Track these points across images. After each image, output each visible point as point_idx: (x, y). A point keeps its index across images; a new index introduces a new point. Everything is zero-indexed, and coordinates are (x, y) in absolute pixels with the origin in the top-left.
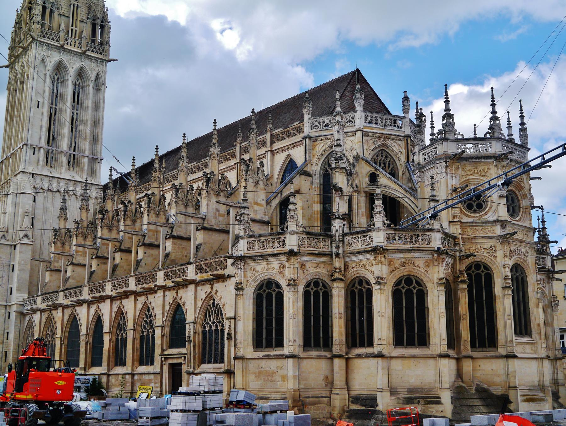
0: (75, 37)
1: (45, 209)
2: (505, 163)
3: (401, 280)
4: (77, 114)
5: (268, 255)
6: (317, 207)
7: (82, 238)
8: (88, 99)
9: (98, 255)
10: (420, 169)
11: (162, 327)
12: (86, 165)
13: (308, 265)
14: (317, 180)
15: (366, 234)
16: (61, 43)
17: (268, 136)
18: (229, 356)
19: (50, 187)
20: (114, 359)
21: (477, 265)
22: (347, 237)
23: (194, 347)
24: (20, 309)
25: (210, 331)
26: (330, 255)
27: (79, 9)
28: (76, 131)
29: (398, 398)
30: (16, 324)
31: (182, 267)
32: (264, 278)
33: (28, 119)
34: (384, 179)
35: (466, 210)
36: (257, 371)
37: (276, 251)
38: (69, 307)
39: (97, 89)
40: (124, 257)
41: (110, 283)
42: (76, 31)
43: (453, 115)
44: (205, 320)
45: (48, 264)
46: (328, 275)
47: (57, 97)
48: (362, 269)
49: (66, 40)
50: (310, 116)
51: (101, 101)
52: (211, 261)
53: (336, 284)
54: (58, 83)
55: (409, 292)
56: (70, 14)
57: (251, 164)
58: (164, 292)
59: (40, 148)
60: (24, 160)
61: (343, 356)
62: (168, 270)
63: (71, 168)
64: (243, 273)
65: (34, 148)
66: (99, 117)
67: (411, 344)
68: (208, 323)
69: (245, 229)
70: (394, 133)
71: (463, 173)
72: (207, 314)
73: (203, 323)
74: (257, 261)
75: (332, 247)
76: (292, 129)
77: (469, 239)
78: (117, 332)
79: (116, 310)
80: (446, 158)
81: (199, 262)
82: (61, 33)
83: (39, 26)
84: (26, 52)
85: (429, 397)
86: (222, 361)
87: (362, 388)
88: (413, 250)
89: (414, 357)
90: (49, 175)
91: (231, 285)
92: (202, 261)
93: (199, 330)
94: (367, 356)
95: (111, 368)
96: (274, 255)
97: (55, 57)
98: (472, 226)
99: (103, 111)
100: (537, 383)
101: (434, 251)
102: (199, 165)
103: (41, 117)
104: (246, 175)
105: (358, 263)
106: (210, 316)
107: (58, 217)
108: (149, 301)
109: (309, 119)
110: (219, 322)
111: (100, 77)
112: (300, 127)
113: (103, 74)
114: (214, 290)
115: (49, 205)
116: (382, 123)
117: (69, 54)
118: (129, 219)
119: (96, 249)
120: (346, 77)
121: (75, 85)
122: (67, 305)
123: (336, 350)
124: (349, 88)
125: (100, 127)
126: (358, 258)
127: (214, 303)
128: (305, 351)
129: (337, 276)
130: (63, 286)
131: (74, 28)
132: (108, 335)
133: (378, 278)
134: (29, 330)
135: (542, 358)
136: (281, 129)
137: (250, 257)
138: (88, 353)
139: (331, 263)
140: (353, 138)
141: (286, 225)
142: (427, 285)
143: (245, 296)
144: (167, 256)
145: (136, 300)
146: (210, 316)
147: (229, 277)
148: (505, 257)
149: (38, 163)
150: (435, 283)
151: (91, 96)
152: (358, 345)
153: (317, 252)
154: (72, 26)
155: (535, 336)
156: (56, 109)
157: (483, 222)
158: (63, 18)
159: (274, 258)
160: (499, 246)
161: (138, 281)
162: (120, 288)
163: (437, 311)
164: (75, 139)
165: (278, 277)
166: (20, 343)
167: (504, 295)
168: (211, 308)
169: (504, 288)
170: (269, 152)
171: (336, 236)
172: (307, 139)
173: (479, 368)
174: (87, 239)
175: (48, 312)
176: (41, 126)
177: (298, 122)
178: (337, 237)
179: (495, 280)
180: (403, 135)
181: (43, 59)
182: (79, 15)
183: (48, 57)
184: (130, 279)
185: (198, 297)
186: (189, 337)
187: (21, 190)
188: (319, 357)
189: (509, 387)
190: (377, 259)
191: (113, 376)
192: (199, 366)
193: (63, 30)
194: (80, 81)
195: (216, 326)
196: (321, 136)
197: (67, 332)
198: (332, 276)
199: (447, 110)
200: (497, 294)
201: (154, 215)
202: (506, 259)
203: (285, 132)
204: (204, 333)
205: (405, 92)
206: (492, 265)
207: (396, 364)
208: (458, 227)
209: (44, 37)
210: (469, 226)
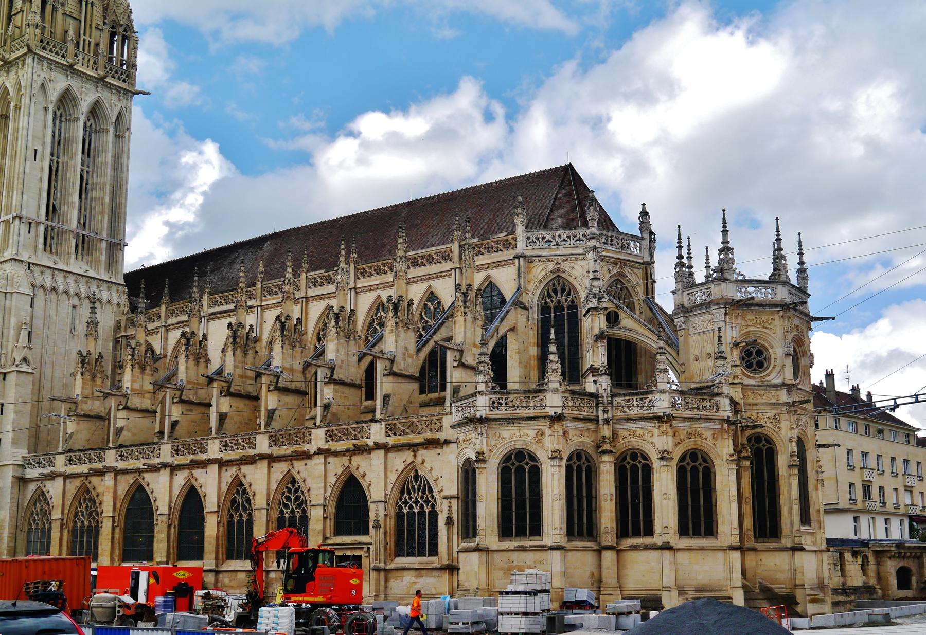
0: (89, 52)
1: (47, 318)
2: (792, 312)
3: (686, 455)
4: (88, 172)
6: (534, 351)
7: (139, 370)
8: (106, 151)
9: (183, 398)
10: (684, 312)
11: (324, 506)
12: (104, 253)
13: (571, 433)
14: (535, 315)
15: (645, 396)
16: (70, 60)
17: (455, 247)
18: (450, 548)
19: (54, 285)
20: (225, 550)
21: (758, 438)
22: (616, 399)
23: (385, 533)
24: (18, 474)
25: (411, 514)
26: (596, 420)
27: (95, 8)
28: (86, 199)
29: (687, 599)
30: (13, 495)
31: (360, 425)
32: (514, 447)
33: (21, 176)
34: (626, 321)
35: (746, 369)
36: (506, 566)
37: (532, 413)
38: (128, 473)
39: (118, 136)
40: (233, 405)
41: (217, 441)
42: (90, 42)
43: (732, 249)
44: (401, 499)
45: (73, 406)
46: (593, 446)
47: (59, 144)
48: (638, 439)
49: (76, 55)
50: (523, 228)
51: (125, 156)
52: (414, 420)
53: (605, 458)
54: (61, 122)
55: (694, 469)
56: (81, 16)
57: (469, 292)
58: (325, 458)
59: (38, 223)
60: (15, 242)
61: (615, 547)
62: (334, 428)
63: (80, 256)
64: (484, 440)
65: (30, 223)
66: (122, 180)
67: (697, 533)
68: (406, 503)
69: (486, 383)
70: (631, 259)
71: (743, 323)
72: (404, 489)
73: (397, 503)
74: (504, 425)
75: (597, 411)
76: (494, 242)
77: (750, 405)
78: (229, 511)
79: (230, 480)
80: (726, 304)
81: (392, 419)
82: (69, 44)
83: (38, 31)
84: (8, 68)
85: (719, 598)
86: (434, 551)
87: (639, 586)
88: (701, 418)
89: (702, 549)
90: (52, 266)
91: (451, 453)
92: (397, 419)
93: (392, 511)
94: (647, 548)
95: (220, 562)
96: (530, 419)
97: (60, 83)
98: (754, 390)
99: (128, 170)
100: (816, 581)
101: (724, 420)
102: (329, 275)
103: (39, 176)
104: (465, 308)
105: (632, 432)
106: (409, 493)
107: (86, 335)
108: (297, 469)
109: (523, 232)
110: (427, 502)
111: (124, 117)
112: (507, 240)
113: (127, 114)
114: (419, 459)
115: (53, 313)
116: (618, 244)
117: (79, 78)
118: (239, 350)
119: (178, 389)
120: (554, 172)
121: (85, 127)
122: (126, 470)
123: (608, 538)
124: (564, 191)
125: (124, 196)
126: (632, 425)
127: (417, 477)
128: (569, 541)
129: (606, 447)
130: (115, 441)
131: (87, 38)
132: (215, 516)
133: (663, 452)
134: (35, 505)
135: (822, 551)
136: (476, 240)
137: (495, 419)
138: (172, 540)
139: (596, 431)
140: (583, 263)
141: (546, 381)
142: (715, 462)
143: (488, 470)
144: (326, 407)
145: (270, 467)
146: (409, 493)
147: (447, 442)
148: (792, 428)
149: (36, 246)
150: (725, 459)
151: (110, 145)
152: (630, 534)
153: (582, 417)
154: (84, 35)
155: (814, 524)
156: (58, 163)
157: (767, 386)
158: (69, 20)
160: (784, 417)
161: (273, 441)
162: (237, 449)
163: (726, 493)
164: (85, 211)
165: (534, 446)
166: (19, 524)
167: (791, 475)
169: (791, 467)
170: (457, 270)
171: (603, 397)
172: (521, 259)
173: (760, 563)
174: (146, 372)
175: (82, 479)
176: (40, 189)
177: (505, 234)
178: (605, 399)
179: (779, 457)
180: (641, 261)
181: (43, 84)
182: (94, 18)
183: (50, 80)
184: (258, 437)
185: (389, 467)
186: (376, 521)
187: (12, 286)
188: (585, 549)
189: (796, 585)
190: (661, 428)
191: (226, 574)
192: (392, 560)
193: (72, 39)
194: (92, 121)
195: (422, 507)
196: (540, 256)
197: (124, 509)
198: (599, 447)
199: (725, 242)
200: (780, 473)
201: (289, 348)
202: (793, 431)
203: (482, 244)
204: (399, 516)
205: (644, 205)
206: (776, 438)
207: (683, 557)
208: (740, 390)
209: (44, 48)
210: (750, 389)
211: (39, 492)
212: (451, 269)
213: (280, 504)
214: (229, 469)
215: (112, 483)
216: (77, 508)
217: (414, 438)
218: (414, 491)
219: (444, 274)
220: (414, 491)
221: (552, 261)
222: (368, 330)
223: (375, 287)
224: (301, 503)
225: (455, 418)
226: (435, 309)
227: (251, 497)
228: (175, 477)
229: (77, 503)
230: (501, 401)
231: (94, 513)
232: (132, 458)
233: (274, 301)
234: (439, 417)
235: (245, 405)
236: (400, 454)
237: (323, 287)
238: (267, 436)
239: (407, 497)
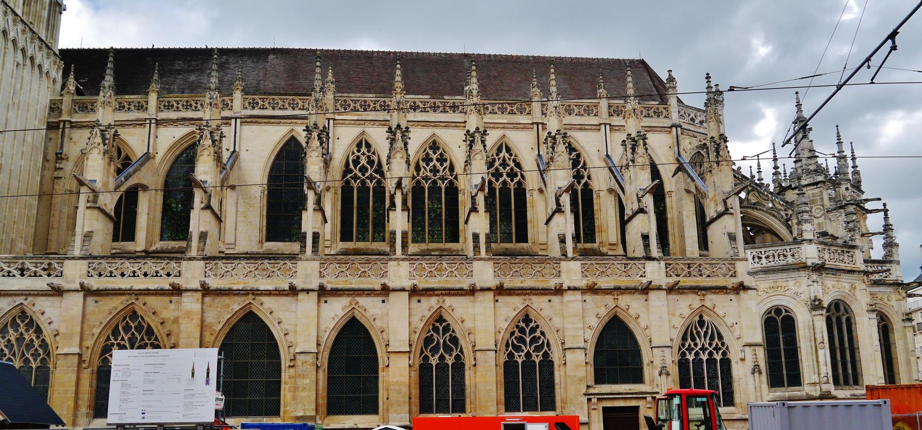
5: (844, 270)
20: (418, 401)
25: (698, 362)
44: (683, 345)
62: (593, 262)
72: (688, 334)
73: (680, 349)
78: (422, 352)
93: (677, 358)
106: (693, 339)
127: (701, 323)
146: (693, 339)
159: (847, 275)
165: (850, 298)
168: (696, 329)
177: (657, 103)
204: (683, 364)
211: (16, 312)
212: (600, 125)
213: (507, 345)
214: (423, 299)
215: (198, 306)
216: (108, 339)
217: (702, 281)
219: (589, 127)
221: (696, 137)
223: (501, 126)
224: (542, 346)
225: (750, 265)
228: (323, 305)
229: (110, 332)
230: (760, 255)
233: (355, 118)
234: (733, 262)
236: (684, 296)
237: (427, 114)
239: (692, 344)
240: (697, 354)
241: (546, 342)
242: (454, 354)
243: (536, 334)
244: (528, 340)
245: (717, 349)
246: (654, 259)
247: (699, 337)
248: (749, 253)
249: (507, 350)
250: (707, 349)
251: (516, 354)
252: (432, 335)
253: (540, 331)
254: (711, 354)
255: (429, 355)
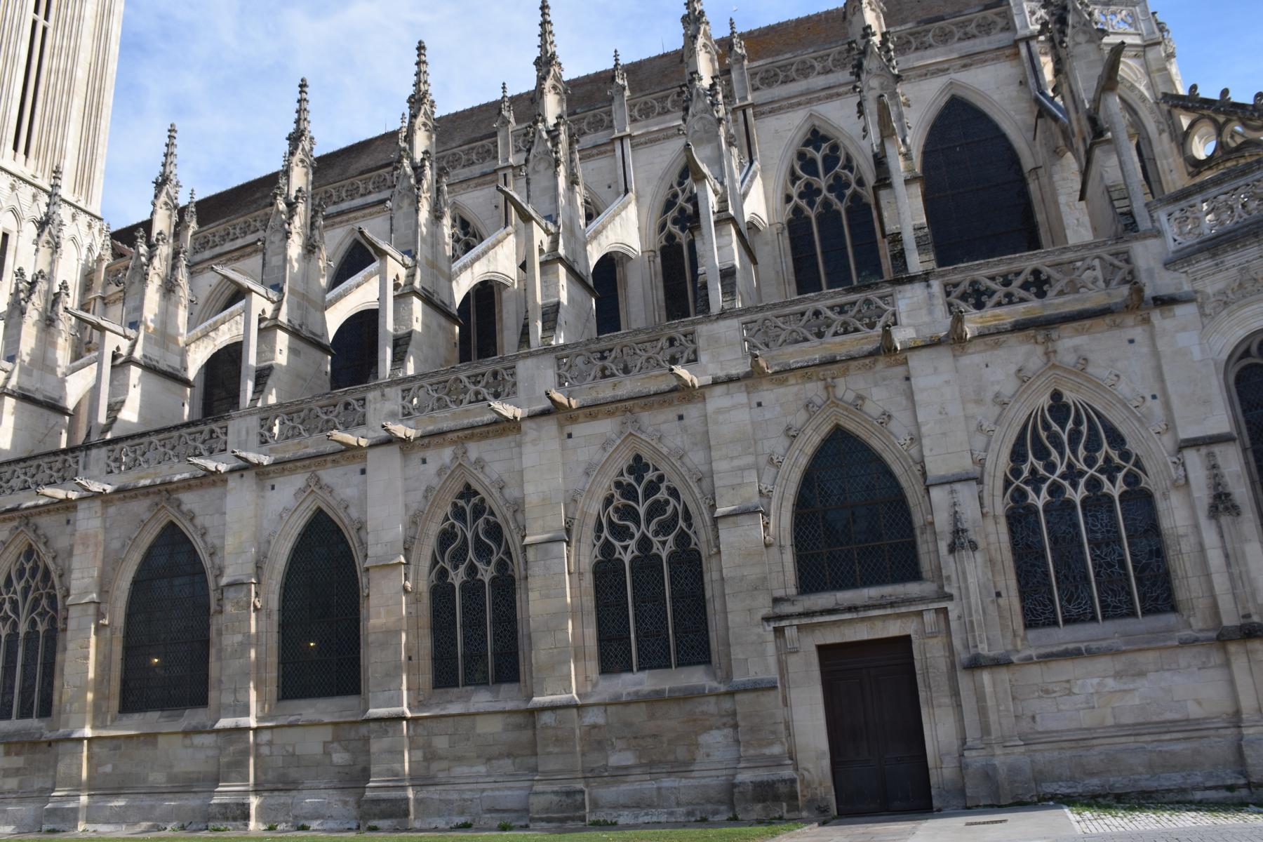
25: (1060, 508)
73: (1007, 483)
78: (435, 562)
91: (1184, 329)
93: (999, 505)
106: (1042, 453)
127: (1059, 408)
168: (1047, 427)
195: (1094, 484)
218: (1059, 445)
220: (1059, 445)
222: (666, 211)
226: (825, 158)
227: (502, 514)
231: (44, 602)
232: (147, 461)
235: (439, 326)
238: (549, 361)
240: (1056, 490)
241: (680, 509)
242: (494, 559)
243: (658, 496)
244: (642, 510)
245: (1110, 470)
246: (912, 279)
247: (1055, 447)
248: (1164, 218)
249: (599, 538)
250: (1082, 474)
251: (617, 544)
252: (453, 526)
253: (668, 488)
254: (1094, 484)
255: (448, 566)
